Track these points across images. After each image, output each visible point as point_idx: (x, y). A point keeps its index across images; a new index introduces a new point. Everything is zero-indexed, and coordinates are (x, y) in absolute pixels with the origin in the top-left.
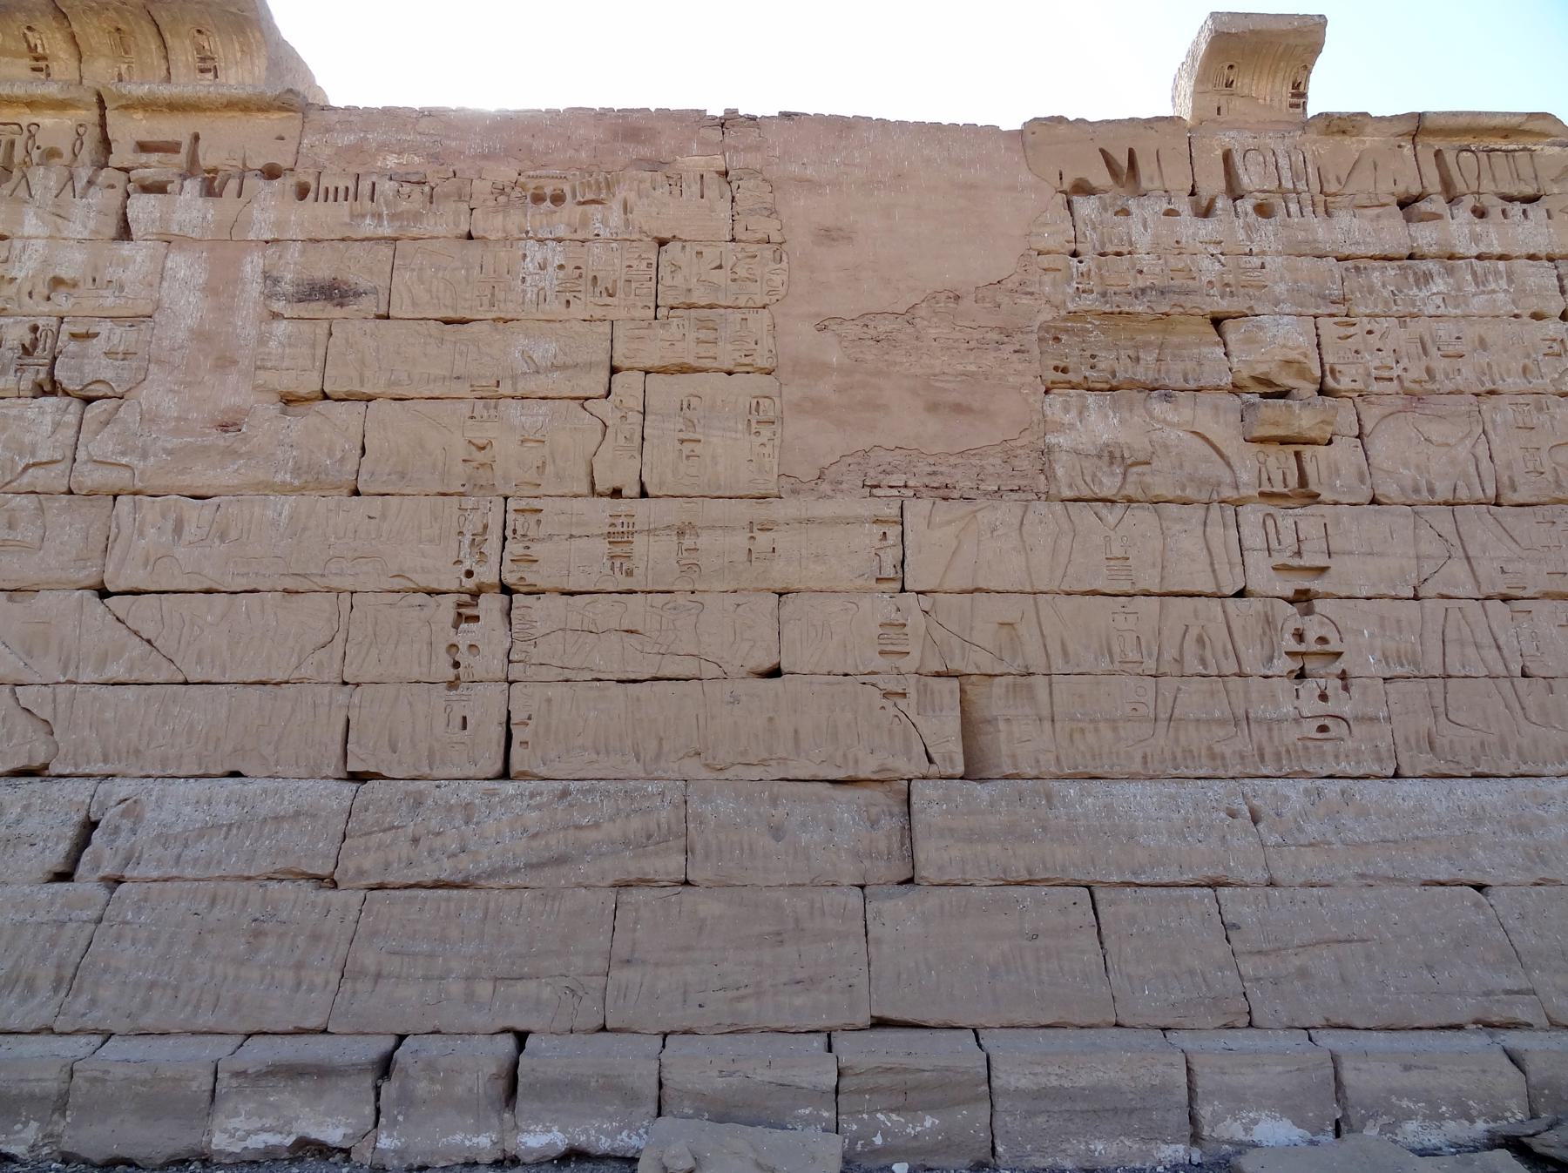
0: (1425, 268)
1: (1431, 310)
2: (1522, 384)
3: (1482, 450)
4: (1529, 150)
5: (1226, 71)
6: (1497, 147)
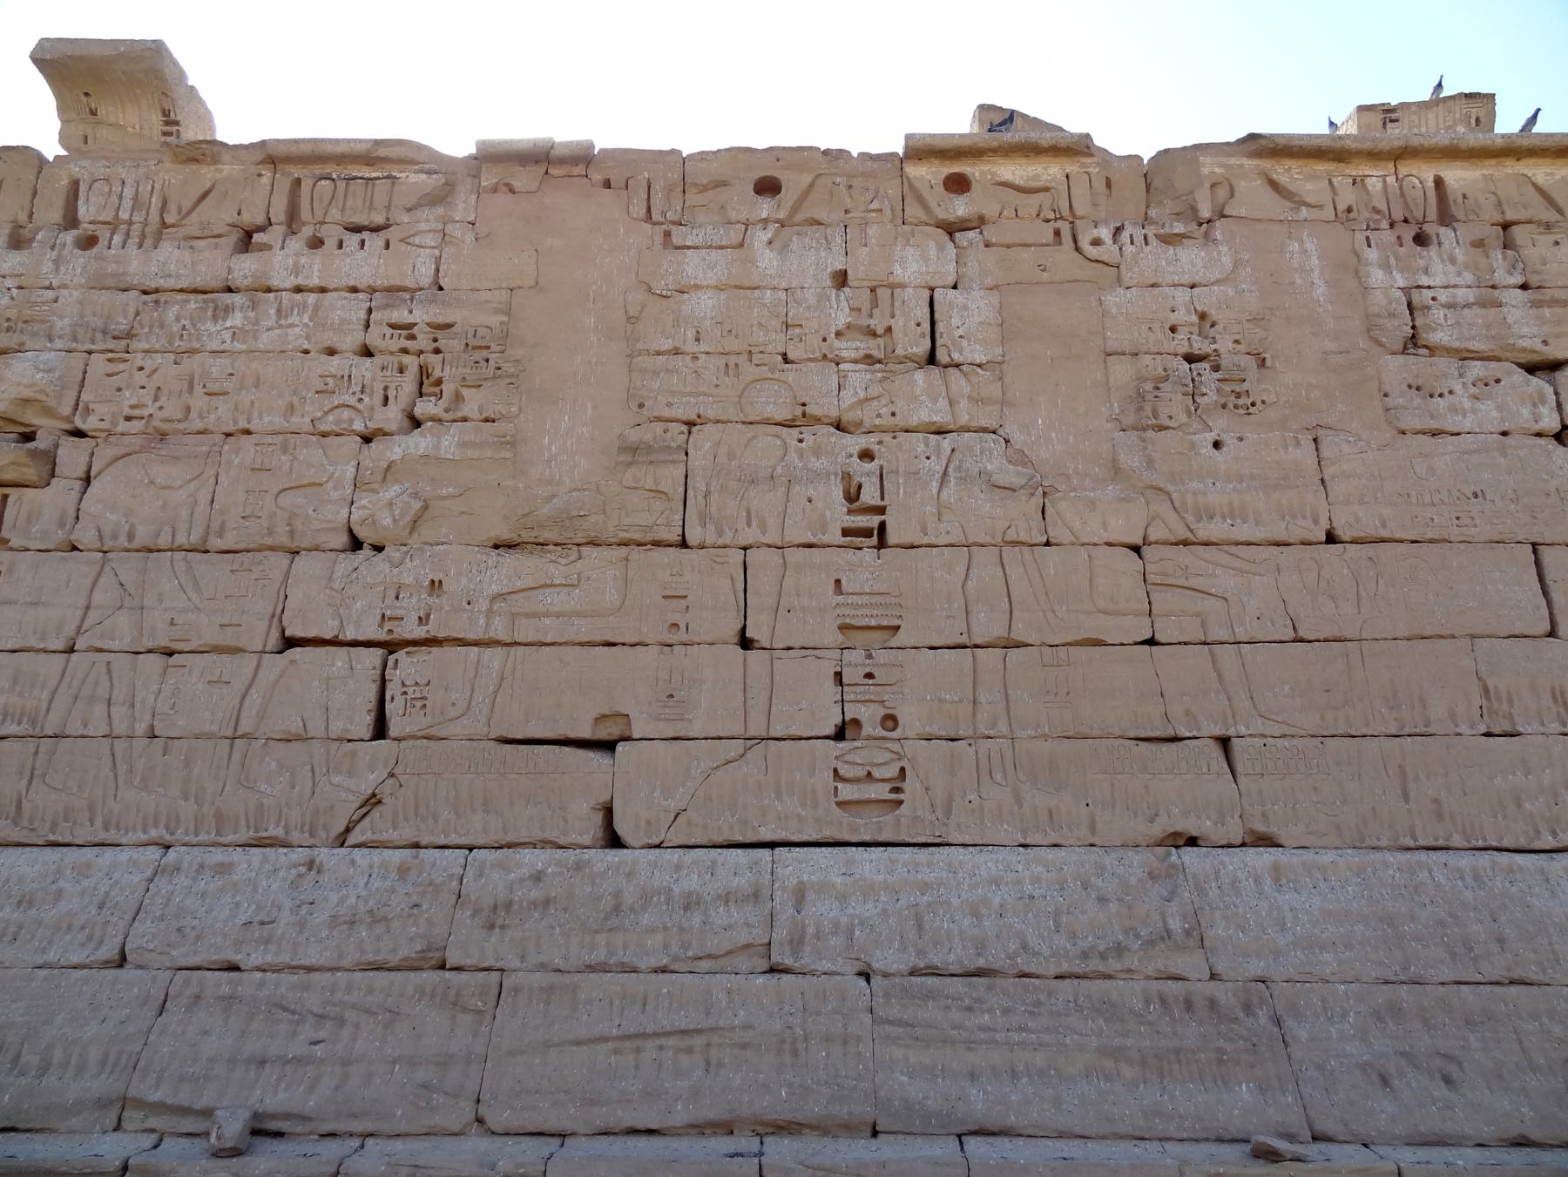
0: (229, 301)
1: (214, 346)
2: (278, 422)
3: (204, 495)
4: (395, 178)
5: (84, 99)
6: (360, 175)
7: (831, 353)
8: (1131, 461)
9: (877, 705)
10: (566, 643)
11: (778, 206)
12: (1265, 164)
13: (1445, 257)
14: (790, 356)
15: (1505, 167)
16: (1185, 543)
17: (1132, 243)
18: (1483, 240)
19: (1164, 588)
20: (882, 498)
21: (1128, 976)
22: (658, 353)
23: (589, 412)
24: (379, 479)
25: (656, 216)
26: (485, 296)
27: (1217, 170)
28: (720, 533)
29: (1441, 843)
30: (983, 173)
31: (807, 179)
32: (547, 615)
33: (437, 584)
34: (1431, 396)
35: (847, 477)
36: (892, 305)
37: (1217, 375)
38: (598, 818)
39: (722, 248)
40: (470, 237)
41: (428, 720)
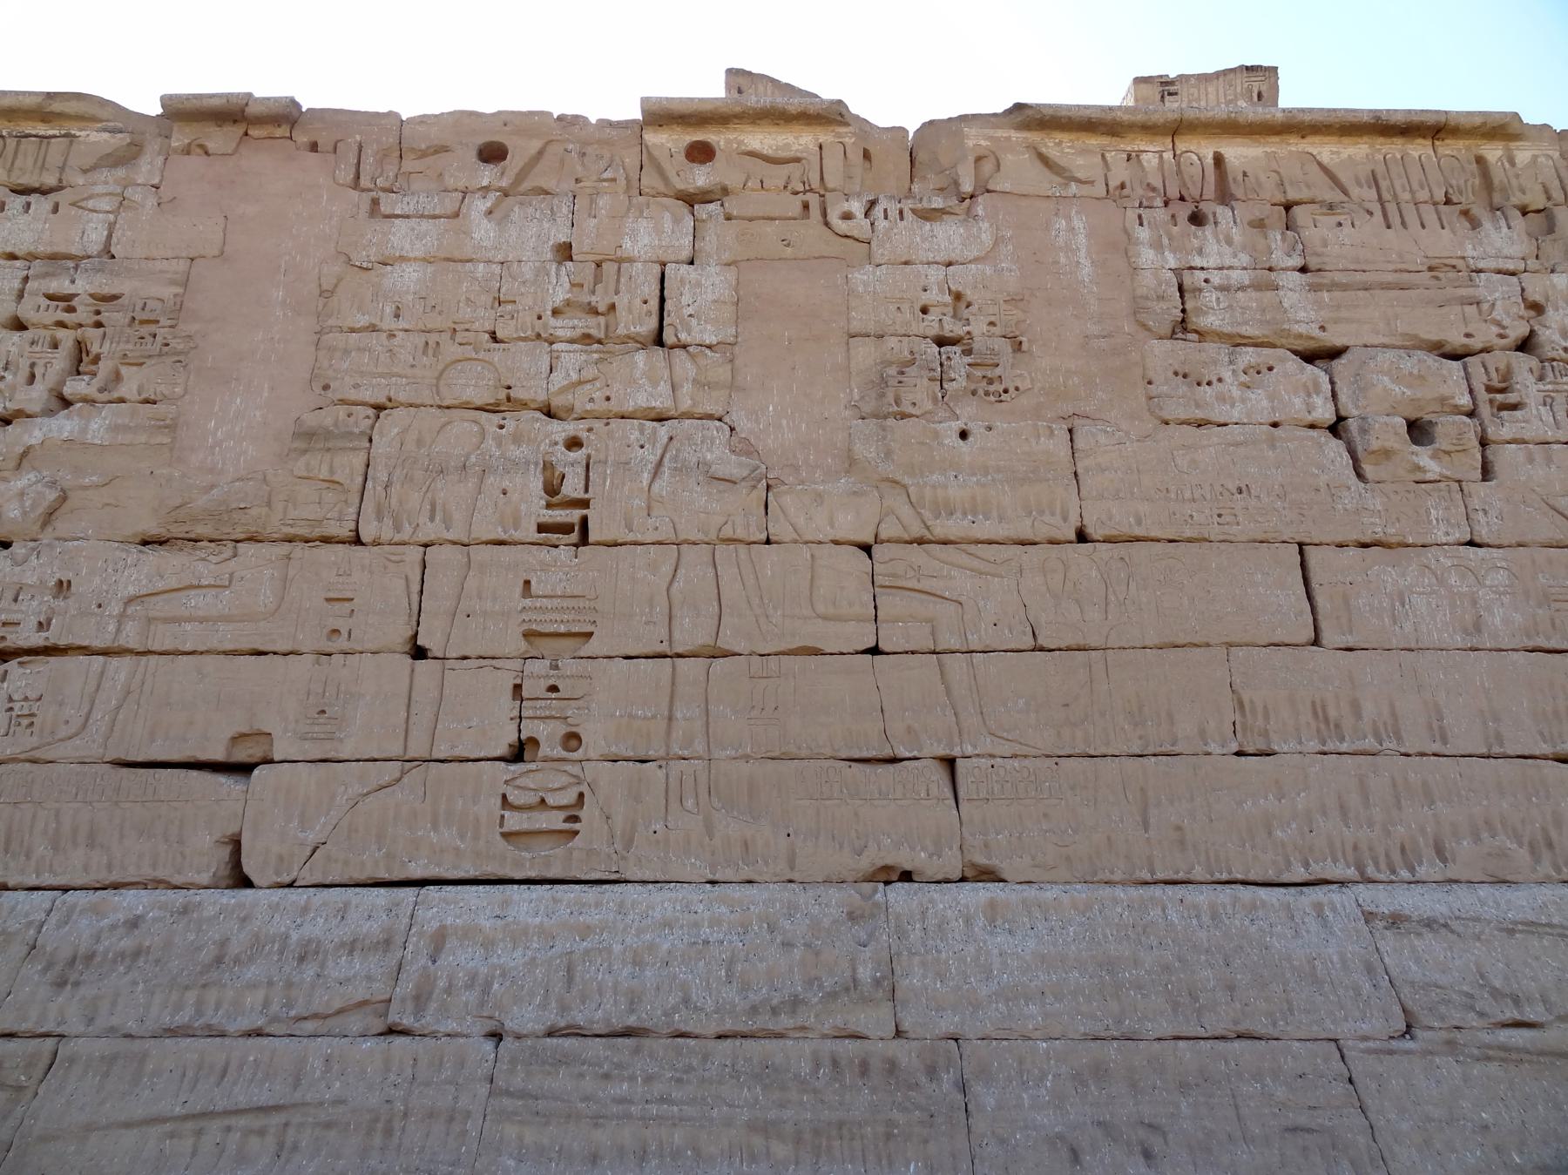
4: (74, 136)
6: (34, 132)
7: (546, 332)
8: (866, 451)
9: (558, 722)
10: (208, 652)
11: (502, 174)
12: (1034, 137)
13: (1221, 237)
14: (499, 335)
15: (1290, 144)
16: (921, 542)
17: (886, 218)
18: (1263, 220)
19: (893, 591)
20: (586, 491)
21: (801, 1035)
22: (353, 330)
23: (266, 394)
24: (12, 464)
25: (365, 182)
26: (164, 265)
27: (983, 143)
28: (398, 528)
29: (1181, 876)
30: (728, 142)
31: (535, 145)
32: (189, 620)
33: (65, 585)
34: (1199, 384)
35: (548, 466)
36: (618, 281)
37: (968, 360)
38: (225, 852)
39: (435, 217)
40: (151, 201)
41: (35, 741)
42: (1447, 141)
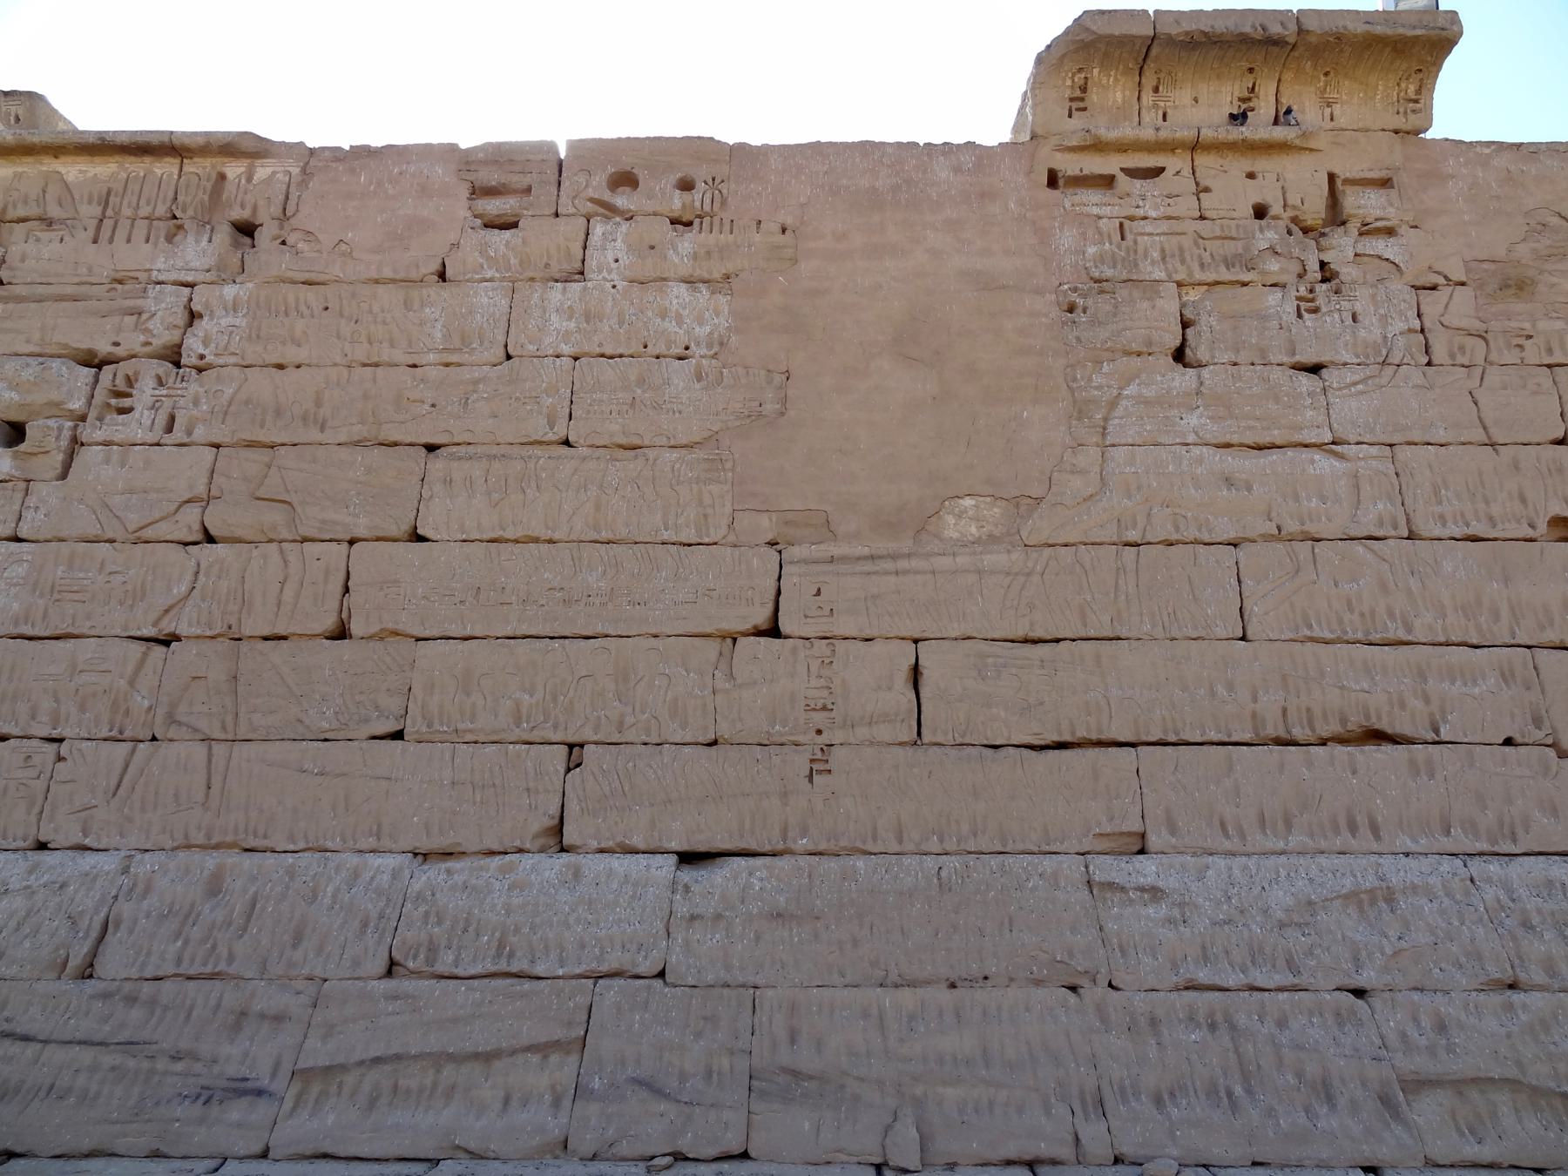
15: (42, 164)
42: (196, 160)
